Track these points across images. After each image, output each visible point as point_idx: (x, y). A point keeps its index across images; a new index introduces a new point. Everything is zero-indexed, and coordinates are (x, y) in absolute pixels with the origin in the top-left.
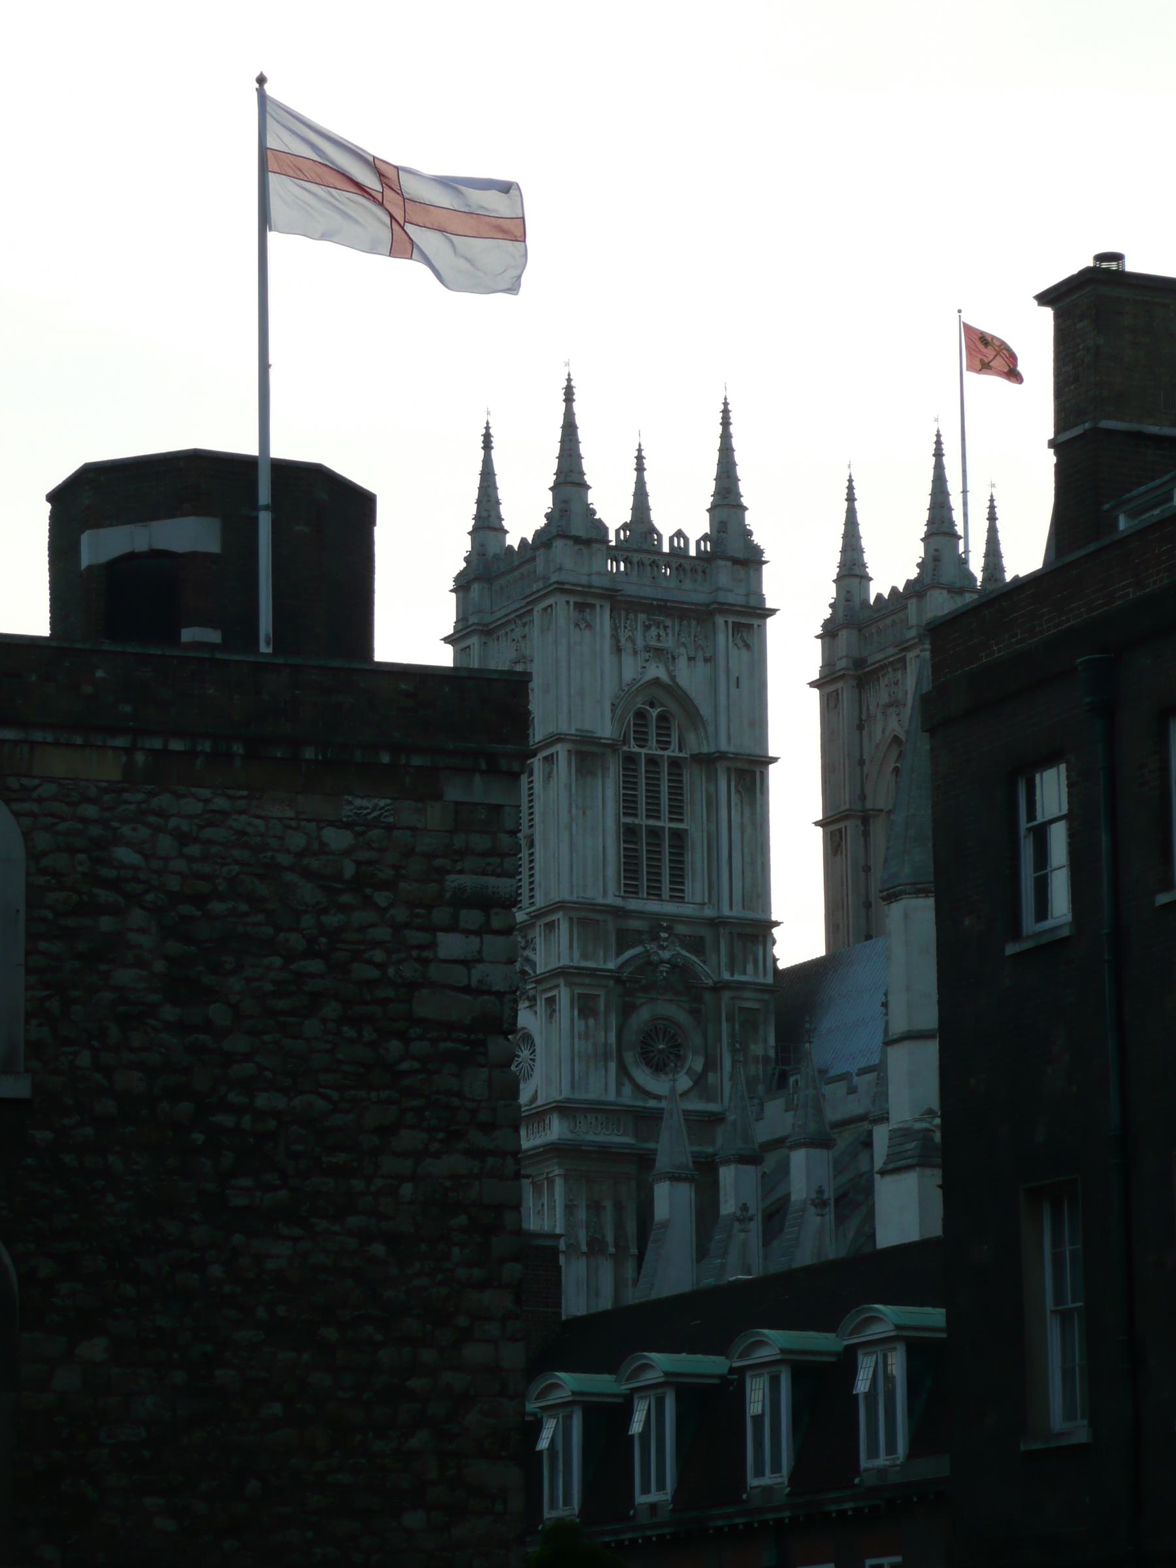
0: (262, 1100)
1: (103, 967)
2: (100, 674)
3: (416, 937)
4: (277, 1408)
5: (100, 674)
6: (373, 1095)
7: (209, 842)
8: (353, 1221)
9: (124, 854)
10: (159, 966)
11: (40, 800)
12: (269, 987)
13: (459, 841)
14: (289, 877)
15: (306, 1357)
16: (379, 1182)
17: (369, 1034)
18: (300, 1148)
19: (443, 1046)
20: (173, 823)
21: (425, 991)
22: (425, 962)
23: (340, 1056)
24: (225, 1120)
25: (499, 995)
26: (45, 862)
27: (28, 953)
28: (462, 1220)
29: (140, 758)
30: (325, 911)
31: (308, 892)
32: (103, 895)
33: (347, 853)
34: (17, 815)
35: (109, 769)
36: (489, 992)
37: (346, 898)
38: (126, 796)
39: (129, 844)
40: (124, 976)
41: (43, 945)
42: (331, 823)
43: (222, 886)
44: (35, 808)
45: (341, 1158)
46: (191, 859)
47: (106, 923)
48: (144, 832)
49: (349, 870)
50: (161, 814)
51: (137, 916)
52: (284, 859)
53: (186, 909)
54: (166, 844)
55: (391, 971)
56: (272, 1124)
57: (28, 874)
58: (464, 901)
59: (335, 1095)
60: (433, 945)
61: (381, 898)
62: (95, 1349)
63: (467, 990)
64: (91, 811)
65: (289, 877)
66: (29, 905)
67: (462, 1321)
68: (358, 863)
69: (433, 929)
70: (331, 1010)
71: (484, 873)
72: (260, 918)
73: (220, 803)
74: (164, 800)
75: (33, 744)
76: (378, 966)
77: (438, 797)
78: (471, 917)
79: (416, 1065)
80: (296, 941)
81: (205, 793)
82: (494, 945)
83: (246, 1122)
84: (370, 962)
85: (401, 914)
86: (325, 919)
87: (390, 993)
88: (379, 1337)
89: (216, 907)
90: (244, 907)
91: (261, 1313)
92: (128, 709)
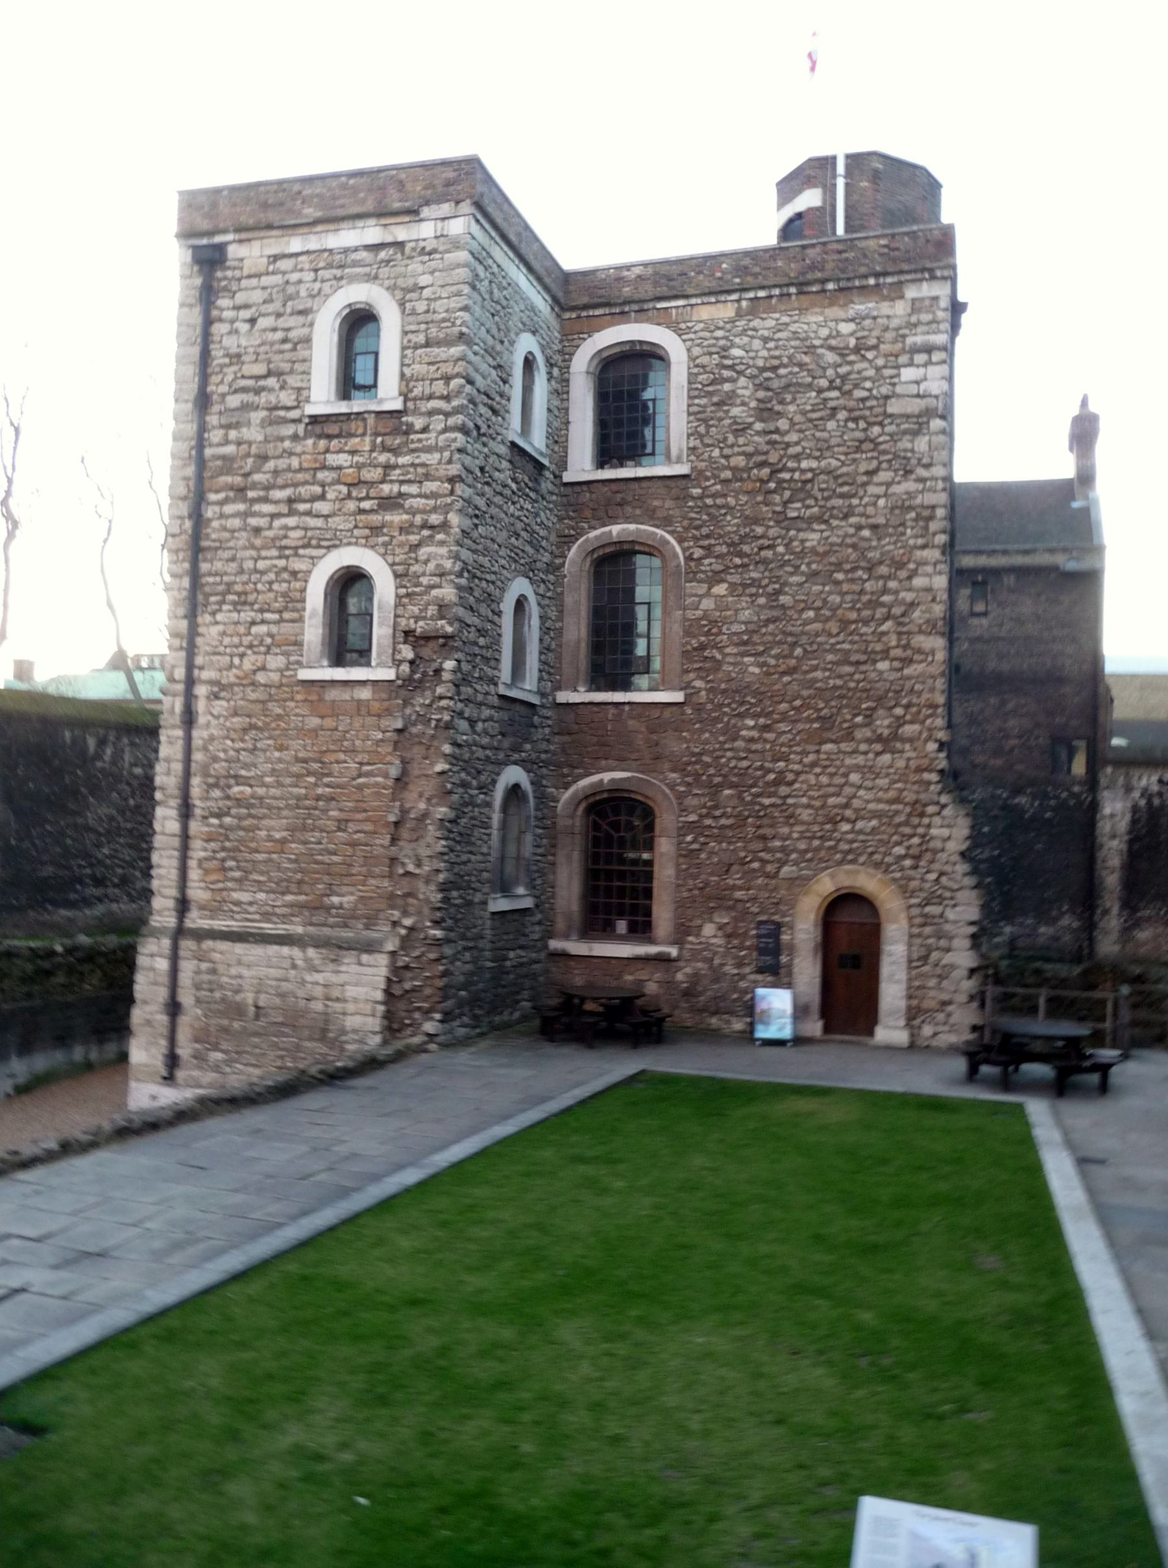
0: (804, 464)
1: (726, 408)
2: (724, 266)
3: (887, 372)
4: (811, 614)
5: (724, 266)
6: (864, 456)
7: (779, 339)
8: (852, 520)
9: (736, 352)
10: (753, 404)
11: (695, 332)
12: (809, 408)
13: (914, 319)
14: (820, 351)
15: (827, 588)
16: (866, 500)
17: (862, 424)
18: (824, 486)
19: (903, 427)
20: (760, 333)
21: (893, 400)
22: (894, 385)
23: (846, 438)
24: (786, 476)
25: (936, 397)
26: (698, 361)
27: (689, 406)
28: (913, 515)
29: (744, 304)
30: (840, 366)
31: (830, 357)
32: (726, 373)
33: (852, 334)
34: (684, 341)
35: (726, 311)
36: (930, 396)
37: (852, 358)
38: (737, 323)
39: (739, 347)
40: (735, 411)
41: (697, 401)
42: (843, 320)
43: (785, 360)
44: (692, 336)
45: (846, 489)
46: (769, 350)
47: (727, 387)
48: (746, 339)
49: (852, 342)
50: (755, 329)
51: (743, 381)
52: (817, 342)
53: (766, 375)
54: (757, 344)
55: (875, 392)
56: (809, 475)
57: (689, 368)
58: (915, 350)
59: (842, 458)
60: (898, 375)
61: (870, 355)
62: (721, 589)
63: (918, 396)
64: (719, 333)
65: (820, 351)
66: (690, 383)
67: (912, 566)
68: (857, 339)
69: (898, 367)
70: (842, 415)
71: (928, 333)
72: (805, 373)
73: (785, 319)
74: (756, 323)
75: (692, 305)
76: (870, 390)
77: (902, 297)
78: (920, 358)
79: (887, 438)
80: (824, 383)
81: (777, 315)
82: (935, 371)
83: (797, 475)
84: (864, 389)
85: (880, 362)
86: (839, 370)
87: (874, 403)
88: (865, 577)
89: (782, 371)
90: (796, 369)
91: (803, 567)
92: (737, 280)
